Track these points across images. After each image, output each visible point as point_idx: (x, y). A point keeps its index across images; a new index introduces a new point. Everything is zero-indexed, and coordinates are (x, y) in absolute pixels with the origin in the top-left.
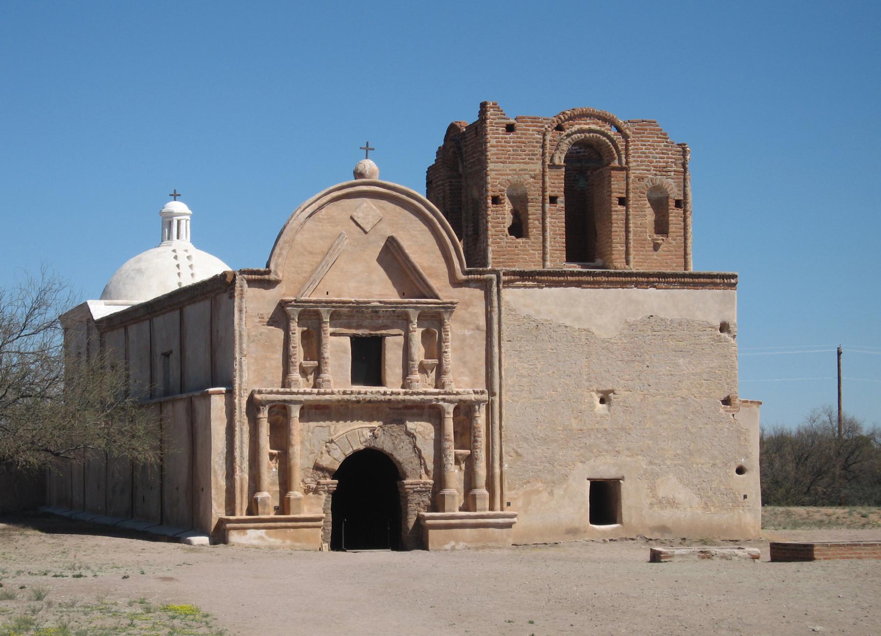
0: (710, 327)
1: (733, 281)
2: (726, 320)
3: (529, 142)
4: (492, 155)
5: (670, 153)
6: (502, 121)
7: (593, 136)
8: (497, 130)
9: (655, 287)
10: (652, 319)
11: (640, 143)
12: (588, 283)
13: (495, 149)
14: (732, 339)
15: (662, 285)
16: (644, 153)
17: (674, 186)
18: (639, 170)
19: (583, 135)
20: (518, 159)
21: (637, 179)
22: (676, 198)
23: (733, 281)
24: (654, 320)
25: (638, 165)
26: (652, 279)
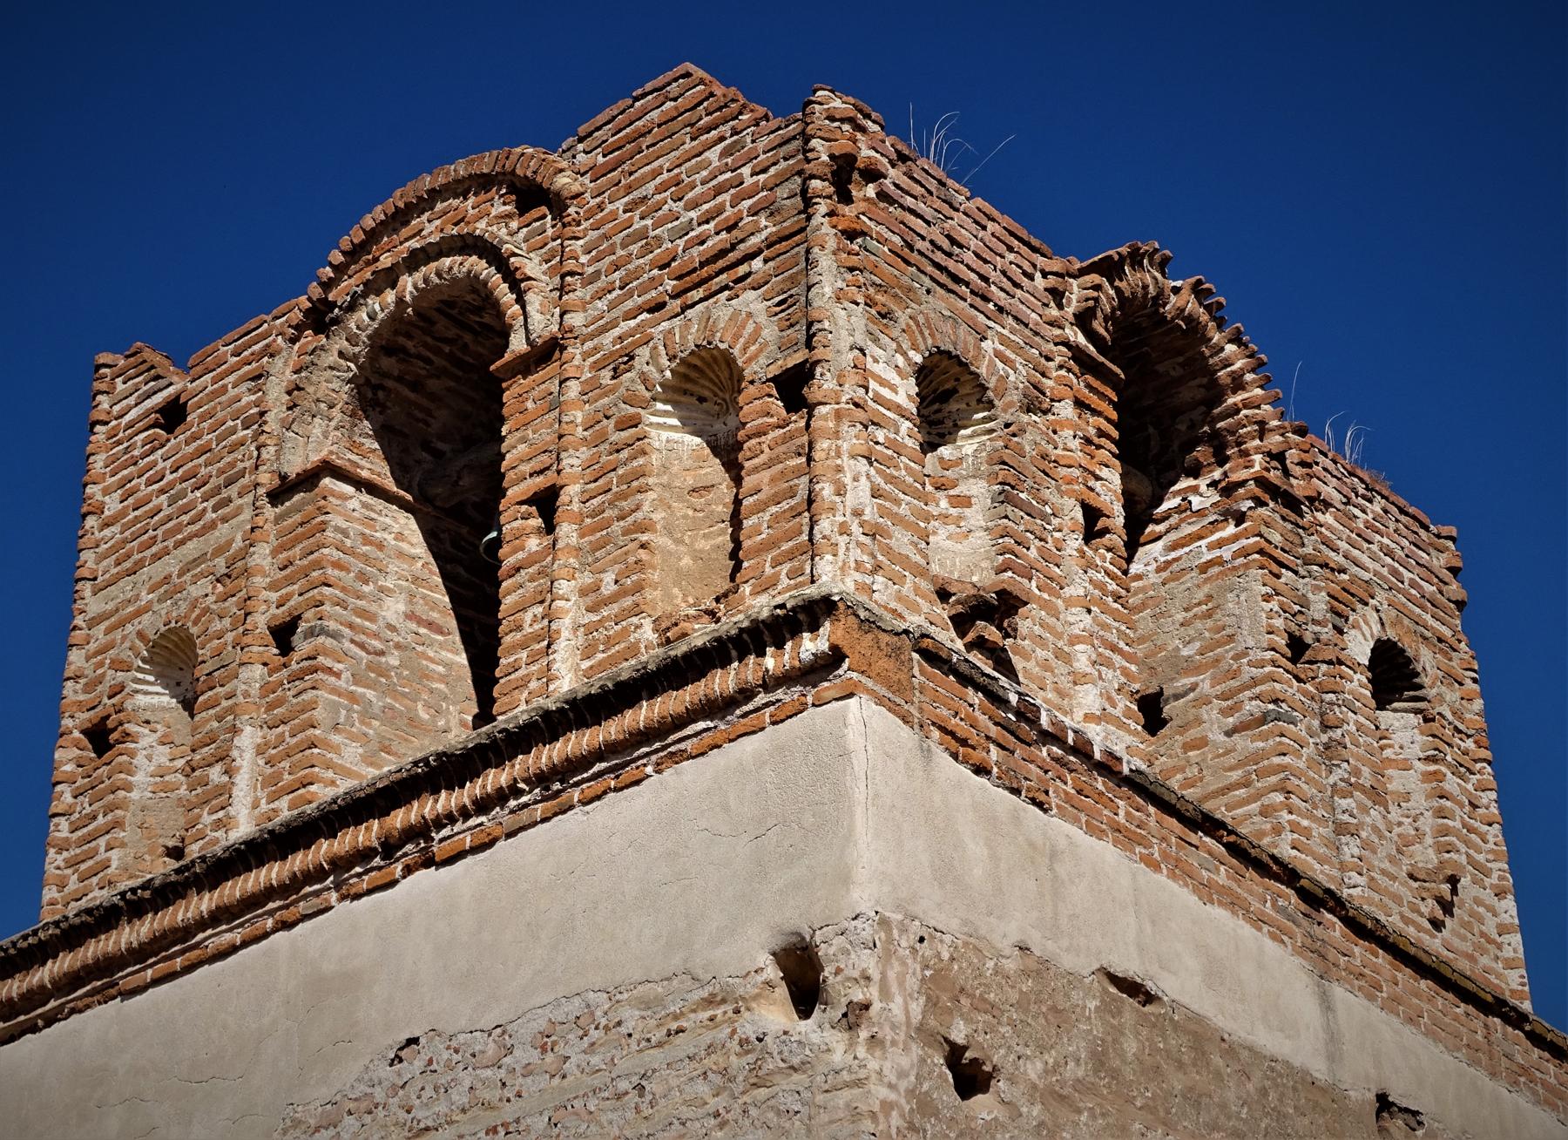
0: (710, 1002)
1: (810, 646)
2: (795, 917)
3: (219, 440)
4: (101, 558)
5: (746, 171)
6: (149, 403)
7: (426, 280)
8: (126, 451)
9: (429, 862)
10: (414, 1064)
11: (620, 205)
12: (139, 954)
13: (116, 529)
14: (837, 1040)
15: (463, 834)
16: (642, 235)
17: (762, 319)
18: (613, 324)
19: (390, 296)
20: (178, 529)
21: (606, 374)
22: (774, 371)
23: (810, 646)
24: (419, 1064)
25: (612, 306)
26: (399, 819)
